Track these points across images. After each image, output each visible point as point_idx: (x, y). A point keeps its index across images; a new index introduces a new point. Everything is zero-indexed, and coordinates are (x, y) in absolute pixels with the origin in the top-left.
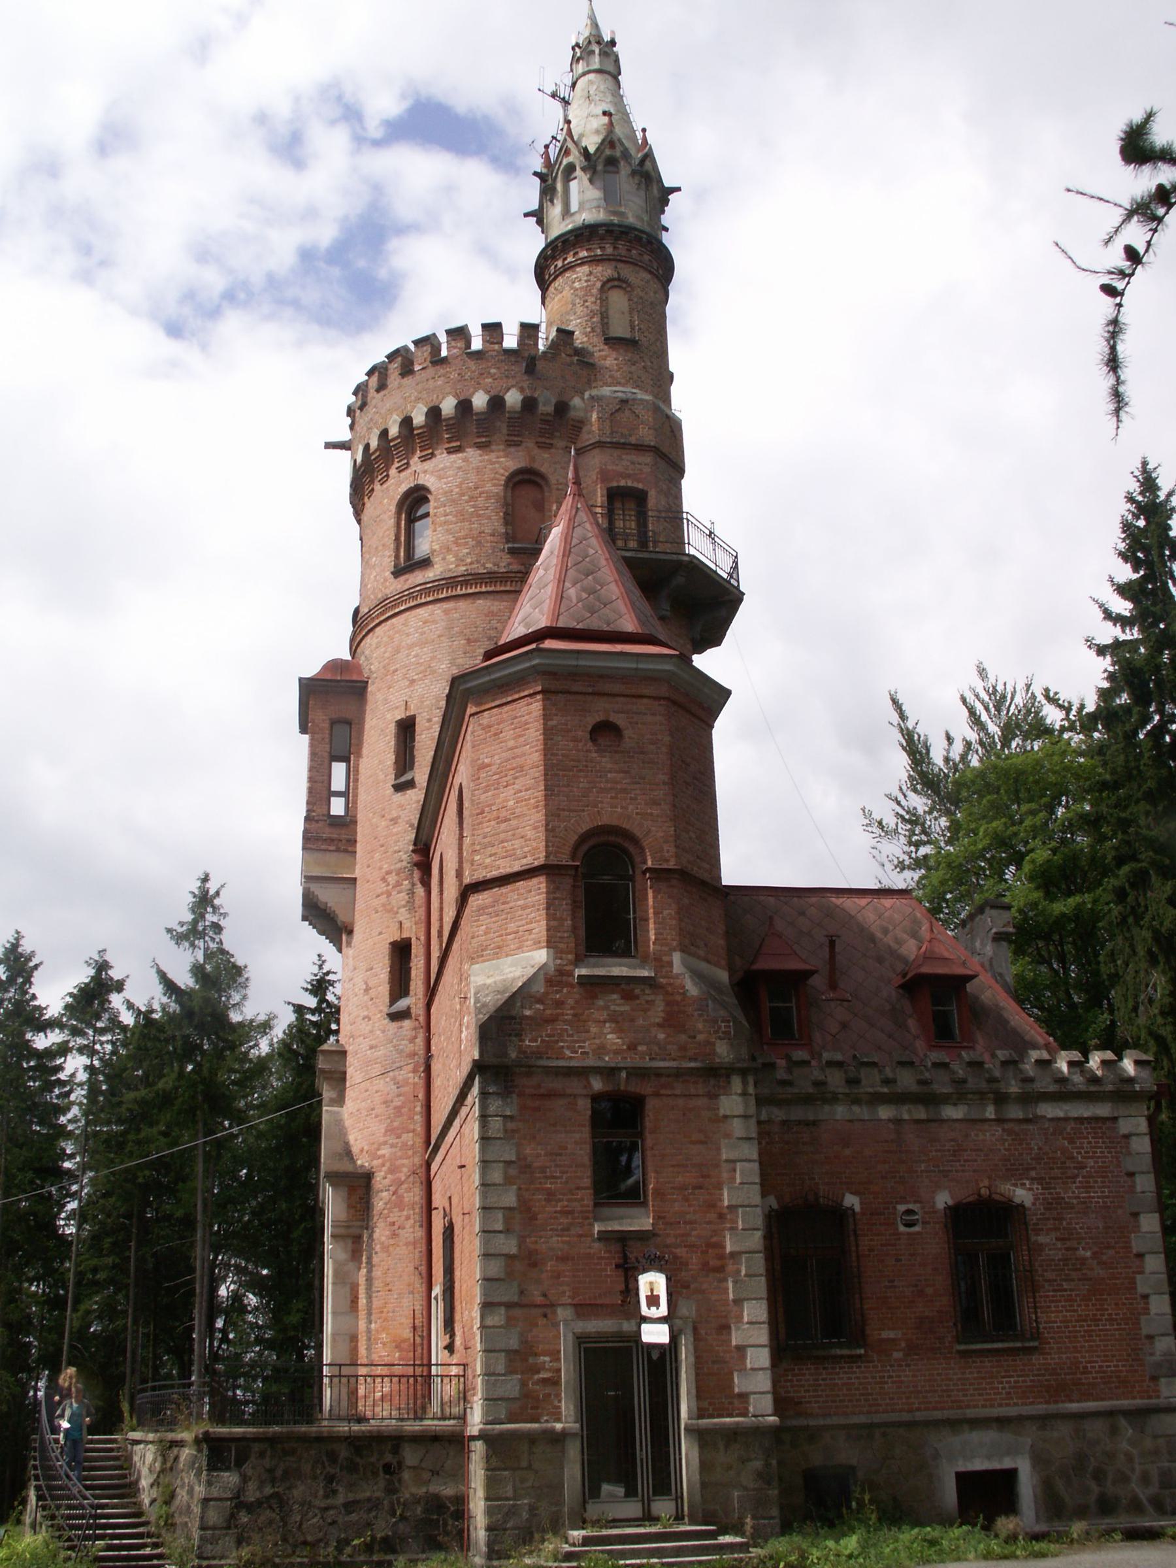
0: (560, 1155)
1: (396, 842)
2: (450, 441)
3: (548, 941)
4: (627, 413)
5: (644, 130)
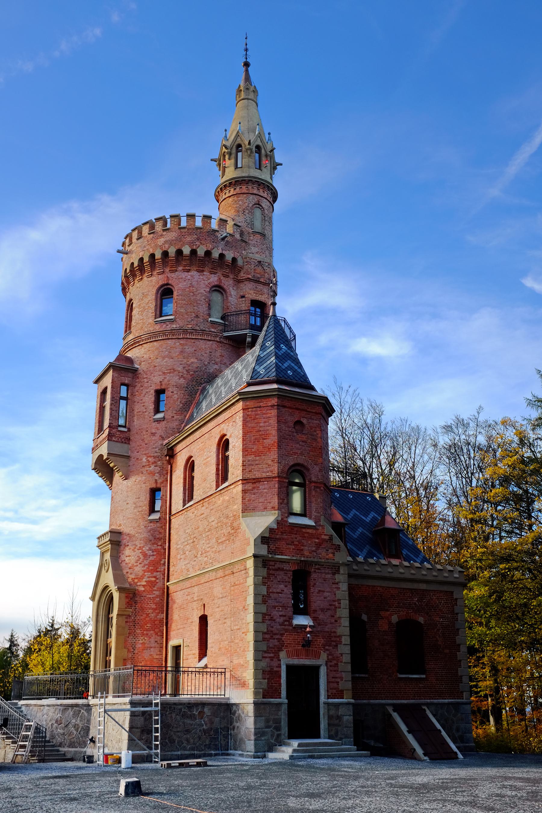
0: (282, 593)
1: (154, 444)
2: (185, 266)
3: (278, 508)
4: (260, 268)
5: (269, 134)
